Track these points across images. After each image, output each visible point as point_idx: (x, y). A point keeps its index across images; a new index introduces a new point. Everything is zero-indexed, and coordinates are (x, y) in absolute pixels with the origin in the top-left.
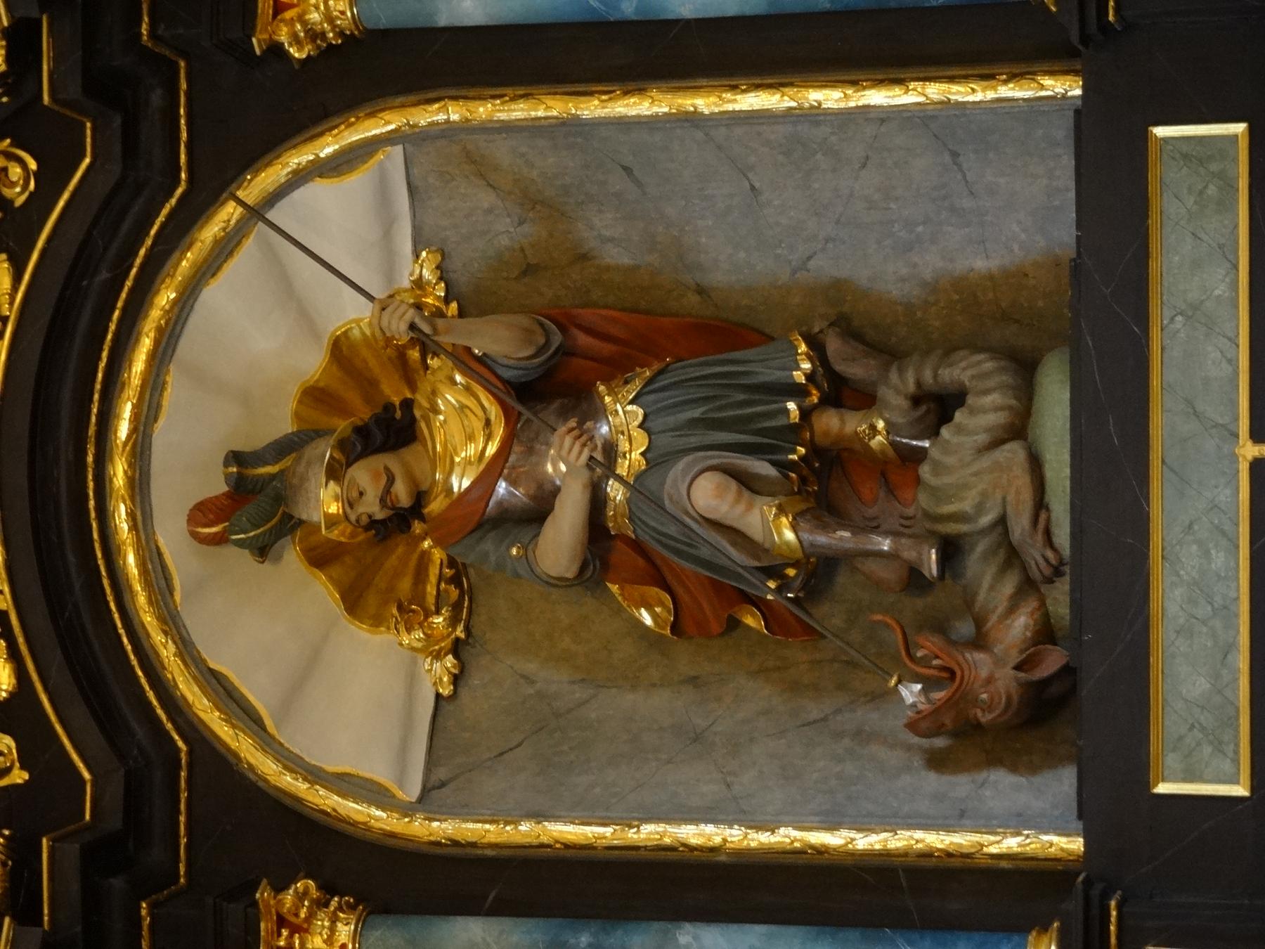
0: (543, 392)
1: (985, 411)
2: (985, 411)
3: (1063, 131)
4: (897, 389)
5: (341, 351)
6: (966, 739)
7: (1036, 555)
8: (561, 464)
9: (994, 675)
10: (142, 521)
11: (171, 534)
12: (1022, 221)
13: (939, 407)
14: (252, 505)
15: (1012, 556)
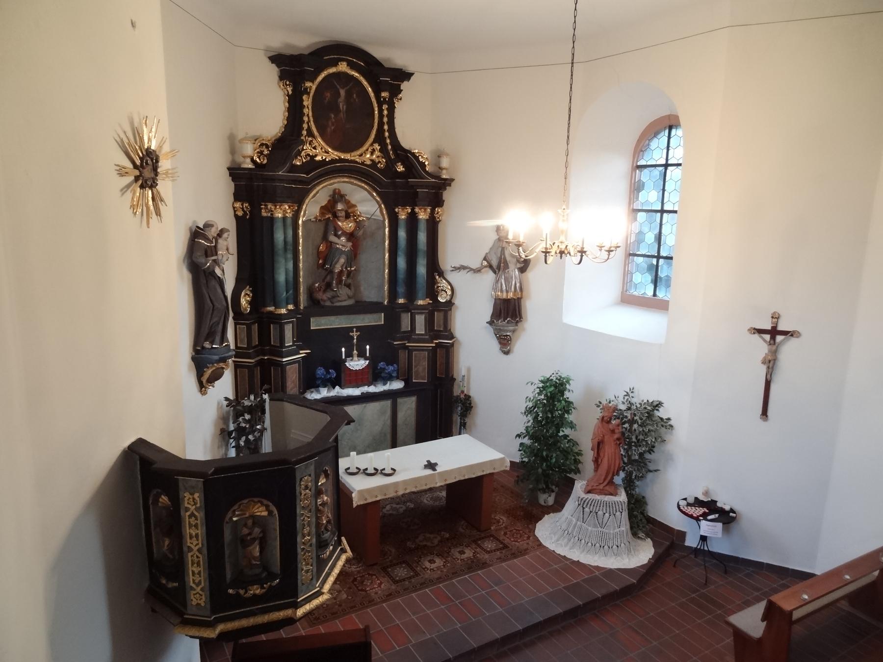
0: (351, 236)
1: (350, 293)
2: (350, 293)
3: (380, 300)
4: (349, 281)
5: (355, 206)
6: (311, 292)
7: (335, 300)
8: (343, 239)
9: (320, 296)
10: (339, 182)
11: (336, 186)
12: (370, 294)
13: (348, 286)
14: (337, 197)
15: (333, 297)
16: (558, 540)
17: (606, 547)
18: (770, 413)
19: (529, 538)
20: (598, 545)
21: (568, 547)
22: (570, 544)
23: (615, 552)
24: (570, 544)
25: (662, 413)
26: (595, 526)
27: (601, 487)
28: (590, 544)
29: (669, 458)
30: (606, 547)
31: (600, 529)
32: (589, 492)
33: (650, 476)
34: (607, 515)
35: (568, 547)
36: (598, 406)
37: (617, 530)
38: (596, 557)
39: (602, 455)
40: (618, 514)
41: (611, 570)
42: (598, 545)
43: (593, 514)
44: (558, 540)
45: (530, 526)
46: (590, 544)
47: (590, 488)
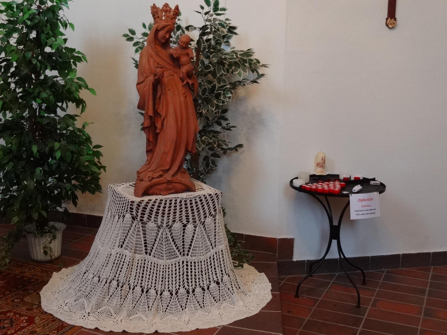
16: (98, 306)
17: (198, 290)
18: (399, 14)
19: (31, 321)
20: (182, 291)
21: (124, 314)
22: (128, 305)
23: (216, 293)
24: (128, 305)
25: (237, 44)
26: (171, 255)
27: (168, 176)
28: (166, 294)
29: (257, 121)
30: (198, 290)
31: (181, 258)
32: (146, 193)
33: (223, 163)
34: (190, 227)
35: (124, 314)
36: (130, 39)
37: (213, 252)
38: (186, 316)
39: (162, 111)
40: (209, 220)
41: (224, 328)
42: (182, 291)
43: (164, 231)
44: (98, 306)
45: (27, 299)
46: (166, 294)
47: (146, 184)
